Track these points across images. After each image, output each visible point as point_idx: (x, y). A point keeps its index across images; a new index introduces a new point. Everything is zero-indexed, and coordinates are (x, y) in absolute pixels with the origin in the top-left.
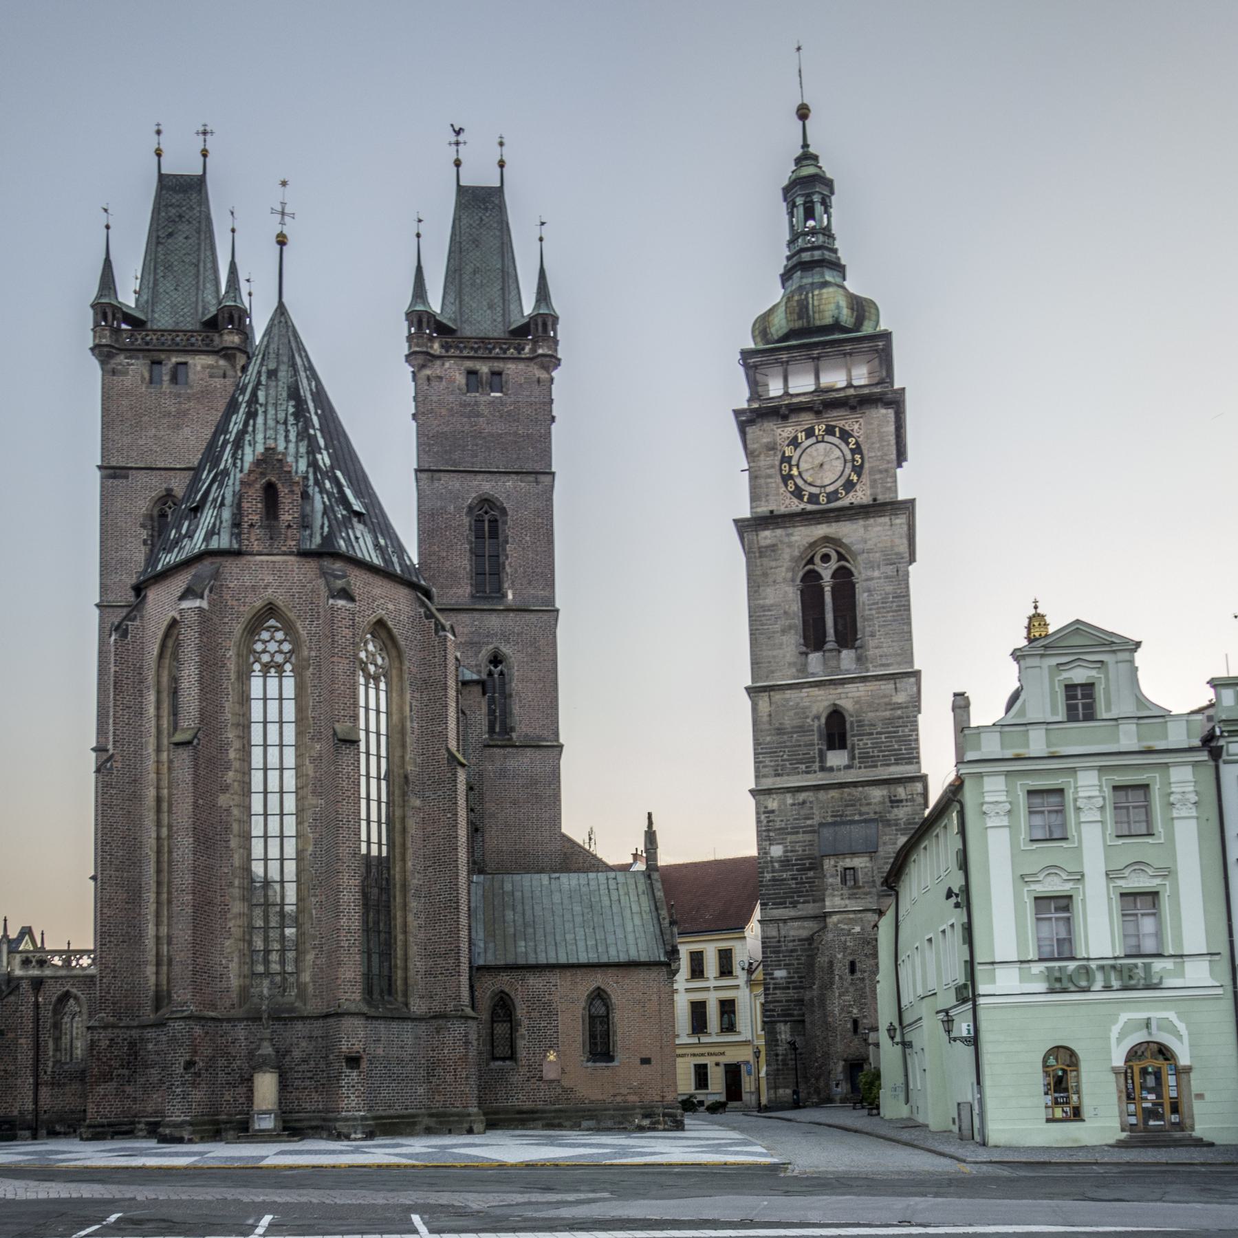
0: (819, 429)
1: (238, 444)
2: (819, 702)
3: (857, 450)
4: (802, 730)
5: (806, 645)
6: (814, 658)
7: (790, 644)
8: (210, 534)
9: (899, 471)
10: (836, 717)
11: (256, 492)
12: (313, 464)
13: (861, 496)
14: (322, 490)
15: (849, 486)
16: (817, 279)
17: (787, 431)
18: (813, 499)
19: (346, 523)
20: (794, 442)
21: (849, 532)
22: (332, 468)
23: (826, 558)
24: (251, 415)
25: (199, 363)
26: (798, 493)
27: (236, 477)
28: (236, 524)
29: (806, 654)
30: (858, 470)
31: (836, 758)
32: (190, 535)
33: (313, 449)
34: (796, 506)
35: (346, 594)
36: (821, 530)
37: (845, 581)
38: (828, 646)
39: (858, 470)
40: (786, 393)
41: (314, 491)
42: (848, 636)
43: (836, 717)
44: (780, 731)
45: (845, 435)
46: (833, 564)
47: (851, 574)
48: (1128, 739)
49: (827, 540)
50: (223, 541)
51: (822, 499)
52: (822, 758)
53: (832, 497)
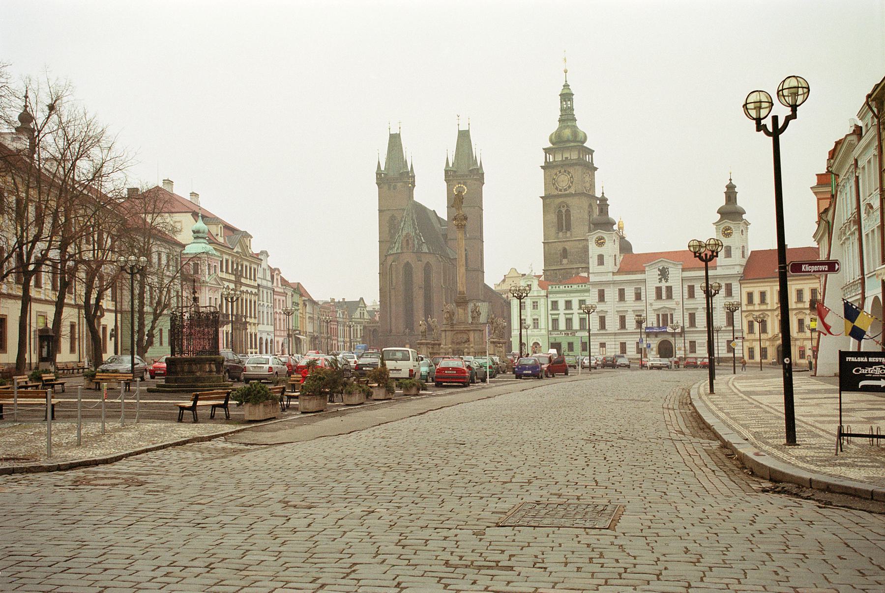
0: (562, 171)
1: (402, 231)
2: (560, 247)
3: (572, 177)
4: (556, 254)
5: (558, 230)
6: (561, 234)
7: (553, 231)
8: (398, 249)
9: (596, 172)
10: (565, 250)
11: (405, 241)
12: (416, 233)
13: (572, 191)
14: (417, 239)
15: (570, 187)
16: (566, 125)
17: (555, 171)
18: (561, 190)
19: (421, 245)
20: (556, 174)
21: (569, 201)
22: (420, 232)
23: (563, 207)
24: (404, 224)
25: (399, 185)
26: (557, 188)
27: (402, 238)
28: (401, 248)
29: (558, 233)
30: (572, 183)
31: (565, 261)
32: (394, 247)
33: (416, 230)
34: (556, 192)
35: (421, 261)
36: (561, 200)
37: (568, 211)
38: (563, 231)
39: (572, 183)
40: (554, 161)
41: (415, 239)
42: (568, 228)
43: (565, 250)
44: (550, 254)
45: (569, 173)
46: (565, 208)
47: (570, 211)
48: (535, 294)
49: (563, 202)
50: (399, 251)
51: (563, 190)
52: (561, 261)
53: (565, 190)
